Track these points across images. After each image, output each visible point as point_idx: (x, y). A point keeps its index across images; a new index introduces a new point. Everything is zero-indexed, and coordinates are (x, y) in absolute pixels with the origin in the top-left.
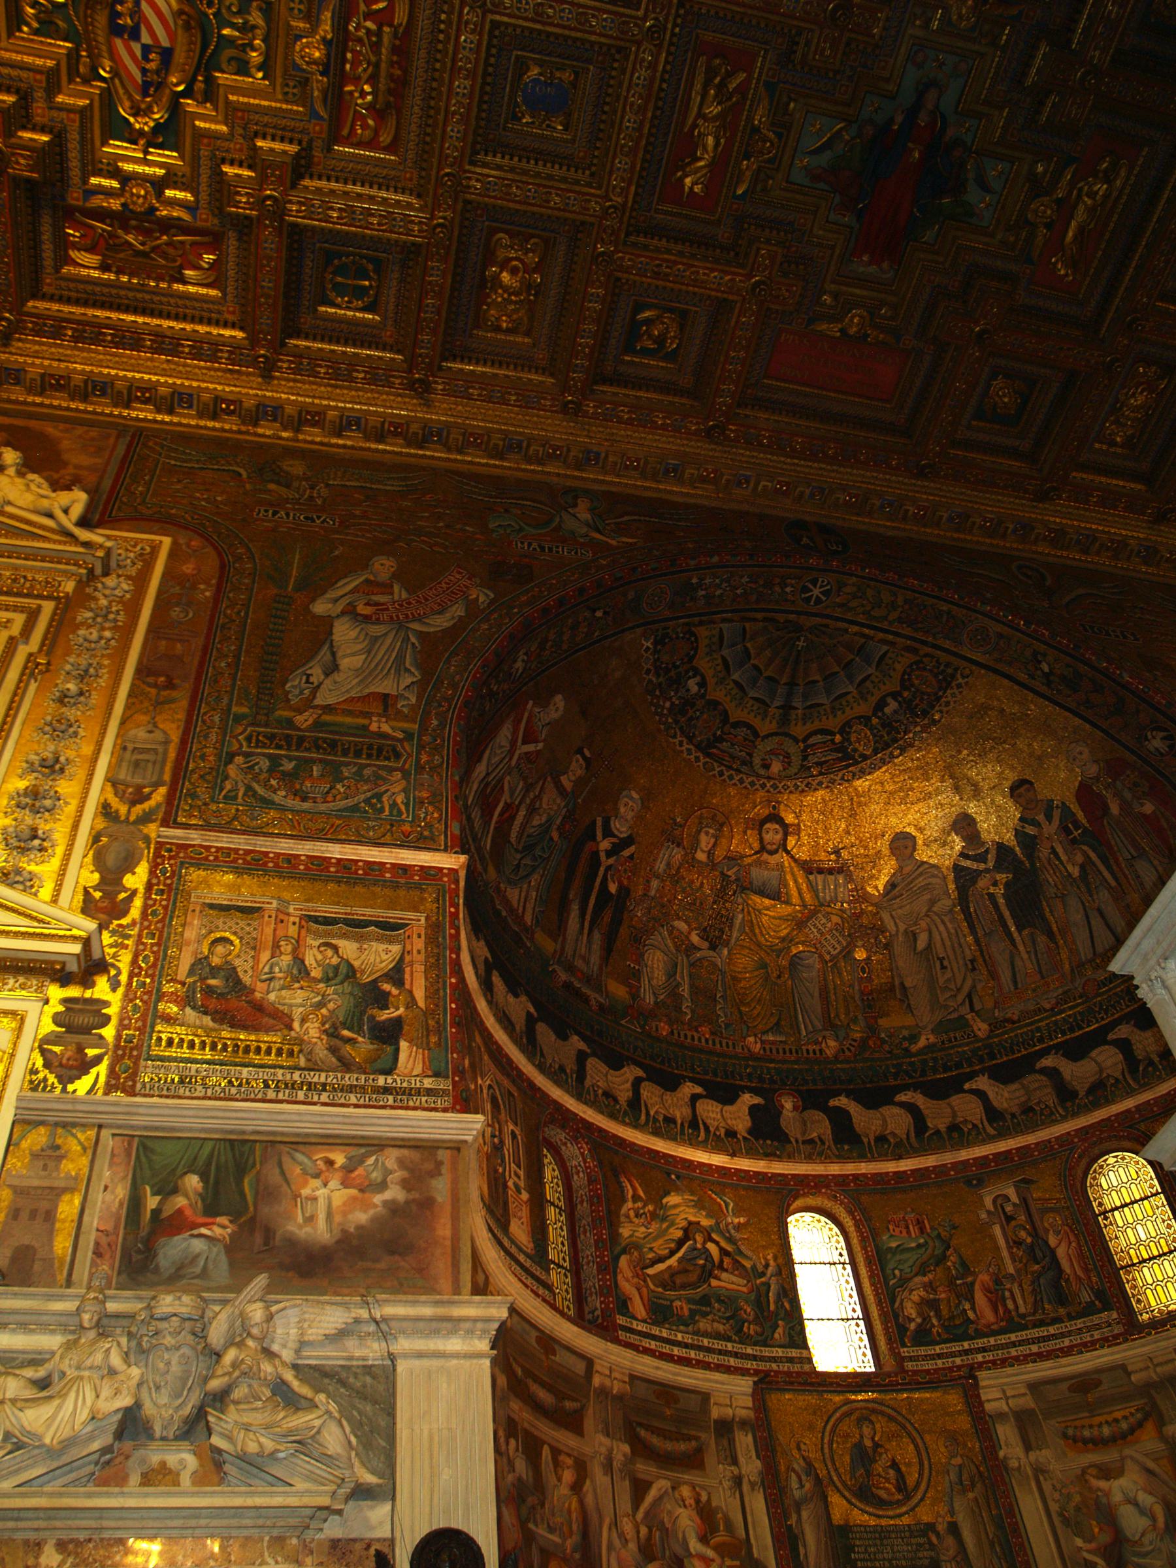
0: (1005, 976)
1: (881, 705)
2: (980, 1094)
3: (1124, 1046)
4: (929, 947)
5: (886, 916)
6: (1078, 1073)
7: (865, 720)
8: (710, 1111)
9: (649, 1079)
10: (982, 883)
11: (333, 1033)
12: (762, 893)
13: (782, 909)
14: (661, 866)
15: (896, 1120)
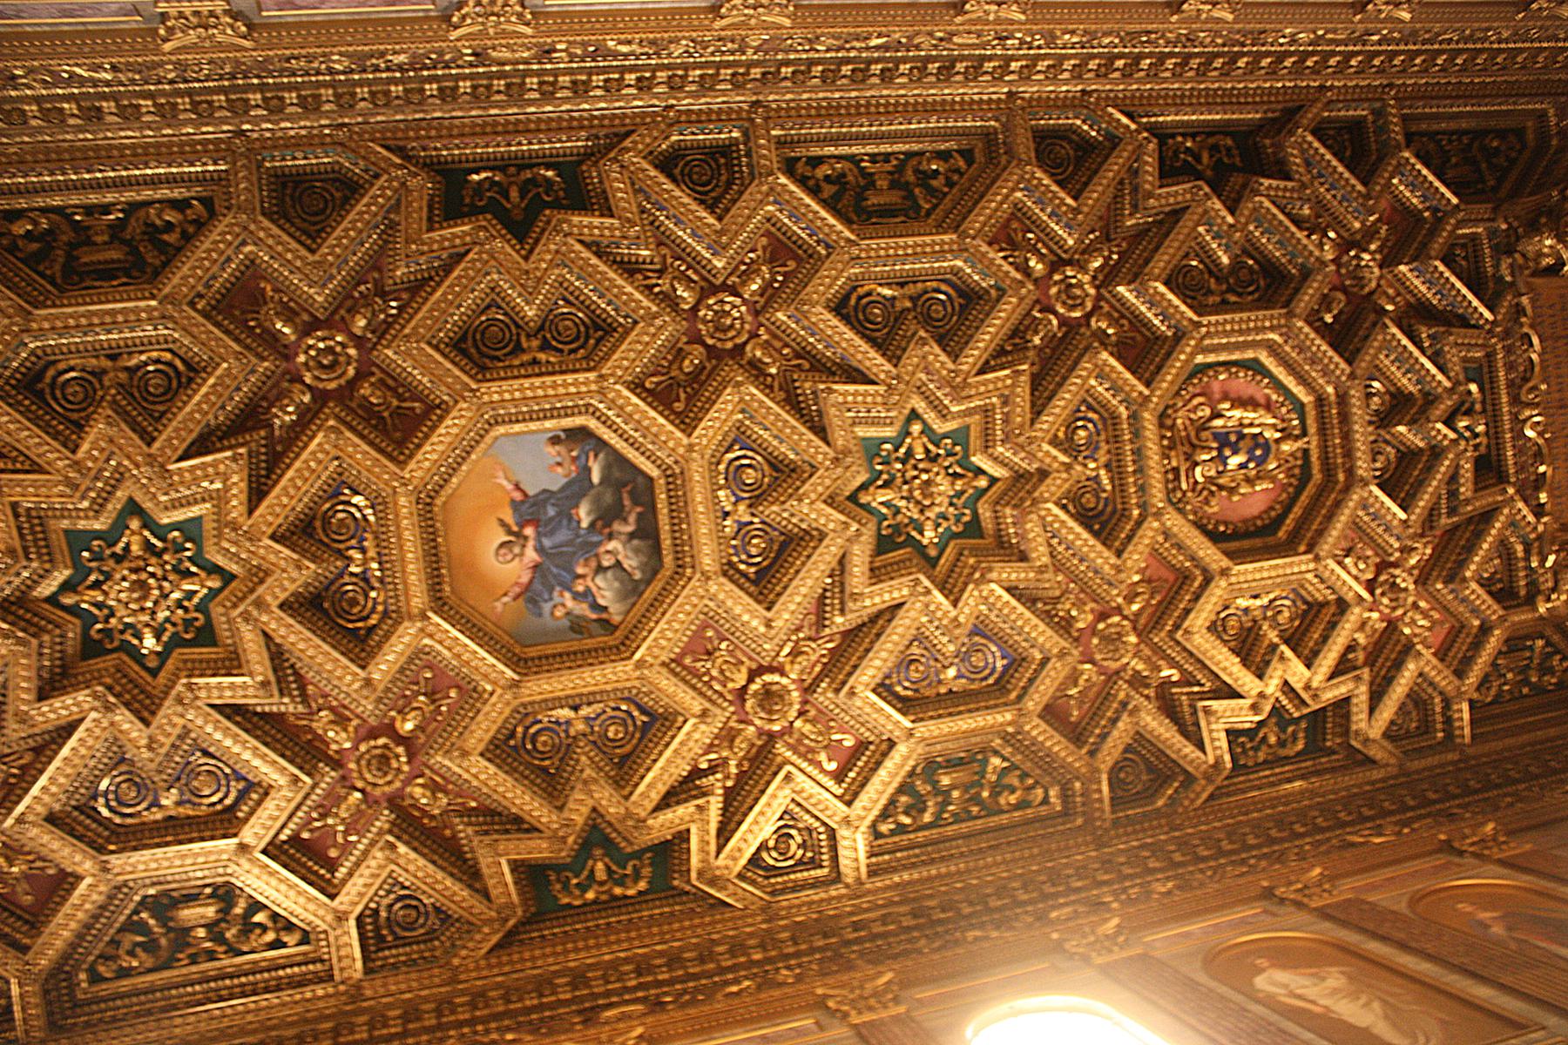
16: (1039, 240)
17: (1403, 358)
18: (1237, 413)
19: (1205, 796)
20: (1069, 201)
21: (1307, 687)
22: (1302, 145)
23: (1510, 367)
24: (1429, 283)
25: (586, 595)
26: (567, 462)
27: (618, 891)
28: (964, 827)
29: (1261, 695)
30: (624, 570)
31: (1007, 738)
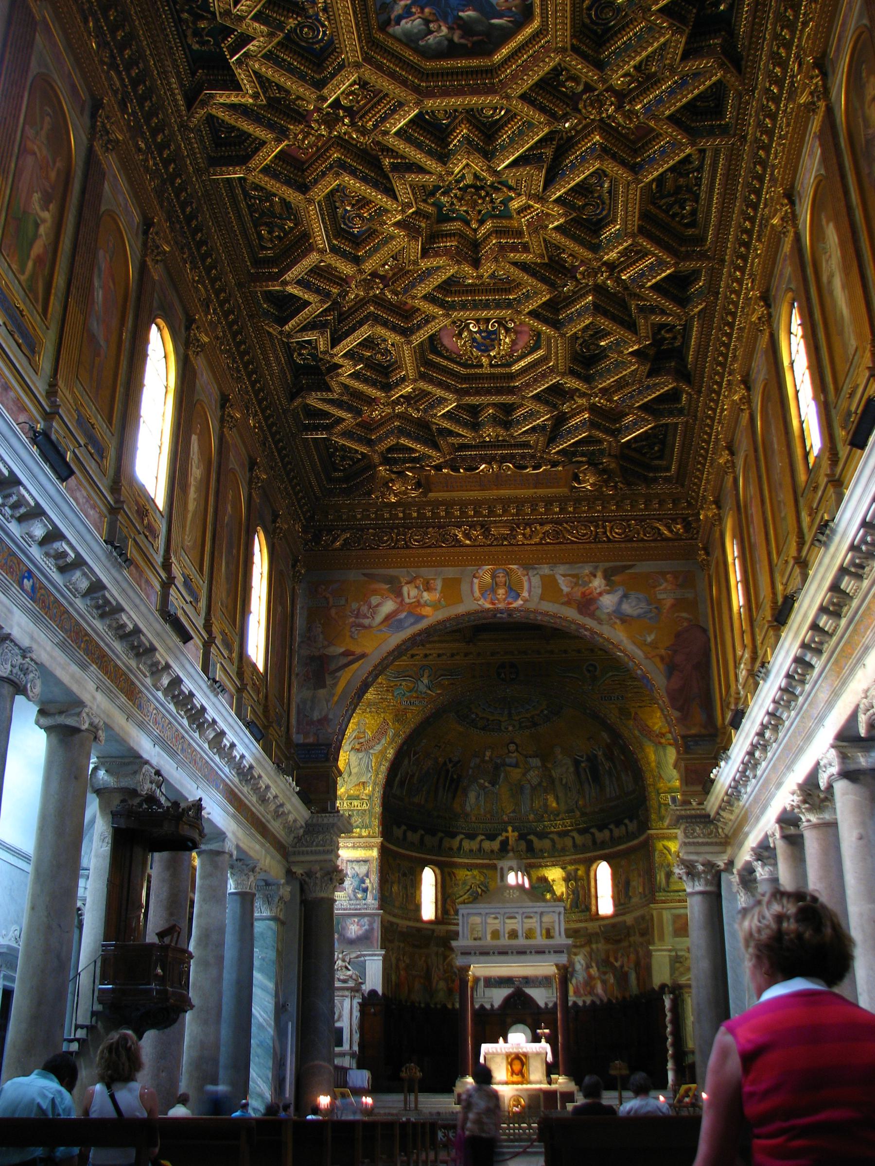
0: (587, 797)
1: (542, 711)
2: (573, 838)
3: (611, 831)
4: (566, 783)
5: (553, 772)
6: (599, 836)
7: (538, 715)
8: (487, 845)
9: (466, 838)
10: (583, 765)
11: (354, 891)
12: (510, 766)
13: (518, 770)
14: (472, 765)
15: (547, 843)
16: (629, 258)
17: (531, 415)
18: (507, 340)
19: (271, 330)
20: (649, 284)
21: (338, 375)
22: (666, 385)
23: (523, 456)
24: (576, 427)
25: (407, 13)
26: (507, 4)
27: (189, 33)
28: (245, 211)
29: (333, 356)
30: (426, 36)
31: (306, 236)
